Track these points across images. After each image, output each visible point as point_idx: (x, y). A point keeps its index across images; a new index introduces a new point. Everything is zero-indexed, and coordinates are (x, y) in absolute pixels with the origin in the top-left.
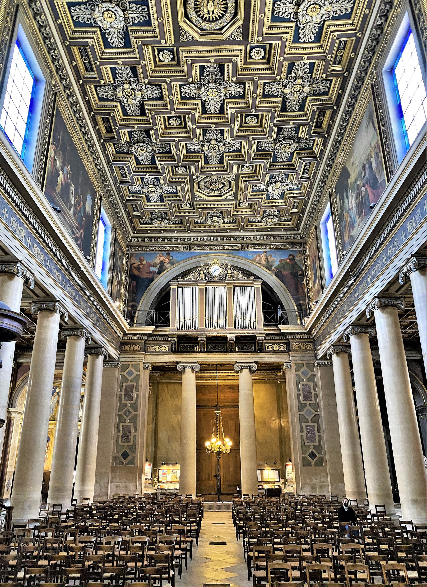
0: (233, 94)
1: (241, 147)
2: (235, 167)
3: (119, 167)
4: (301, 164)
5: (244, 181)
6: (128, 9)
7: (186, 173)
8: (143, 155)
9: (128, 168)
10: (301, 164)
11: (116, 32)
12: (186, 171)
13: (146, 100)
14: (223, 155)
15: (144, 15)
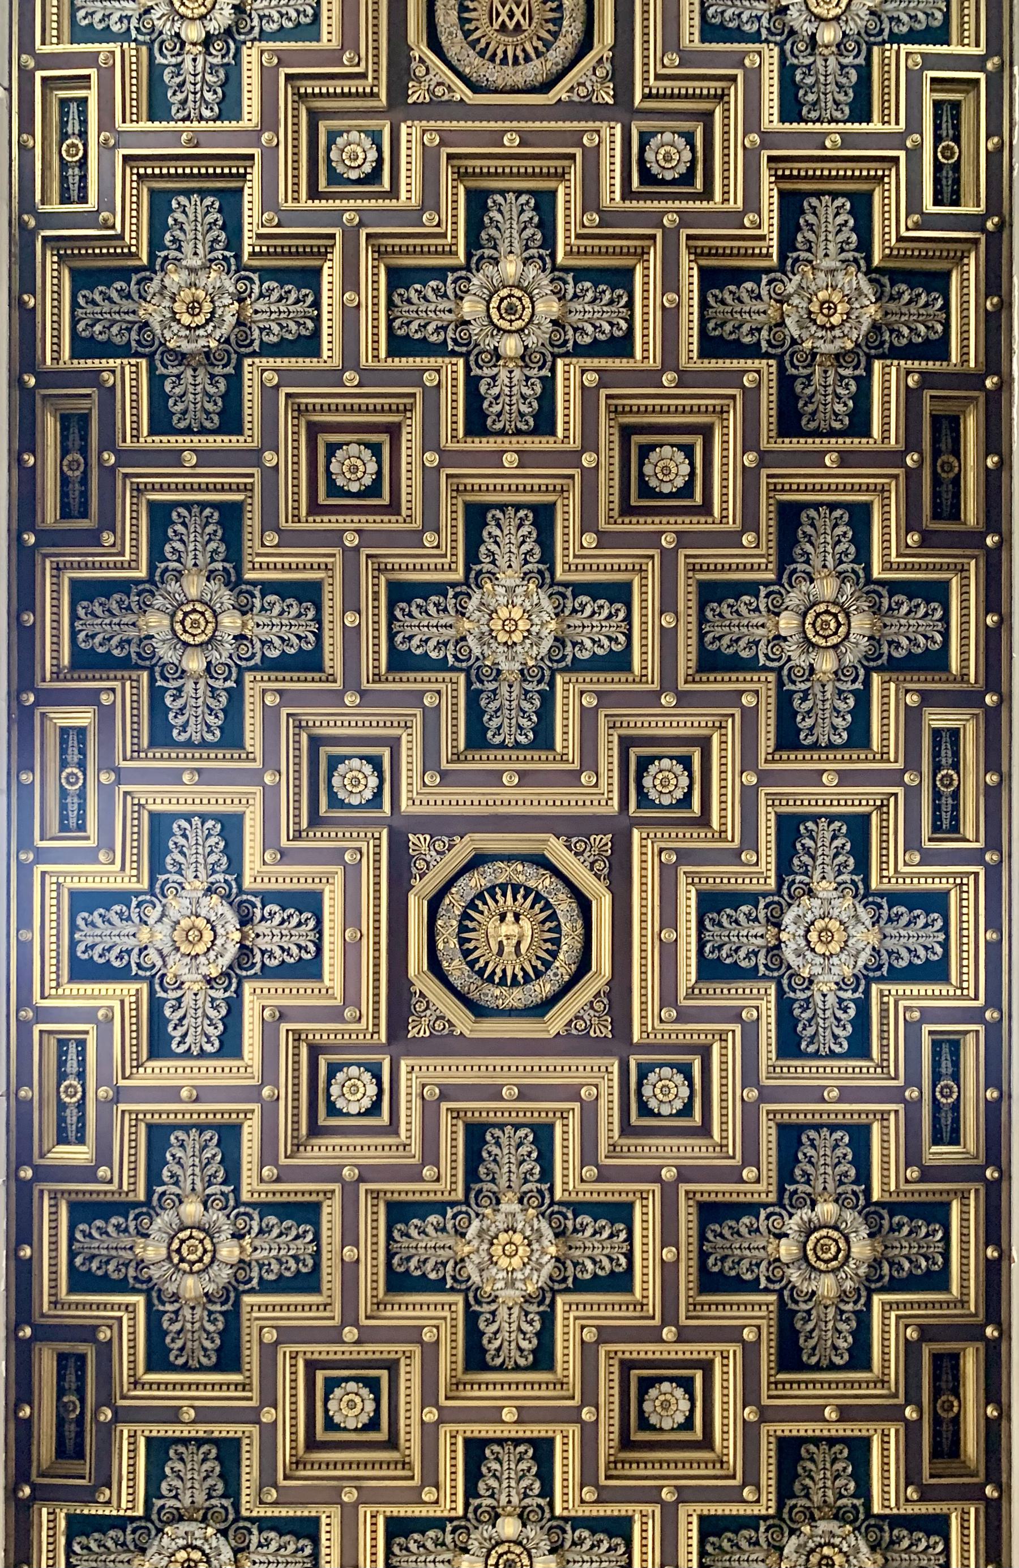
0: (432, 610)
1: (390, 304)
2: (409, 194)
3: (956, 203)
4: (106, 201)
5: (363, 76)
6: (763, 952)
7: (648, 125)
8: (831, 272)
9: (914, 204)
10: (106, 201)
11: (817, 875)
12: (645, 139)
13: (767, 584)
14: (469, 256)
15: (721, 308)
